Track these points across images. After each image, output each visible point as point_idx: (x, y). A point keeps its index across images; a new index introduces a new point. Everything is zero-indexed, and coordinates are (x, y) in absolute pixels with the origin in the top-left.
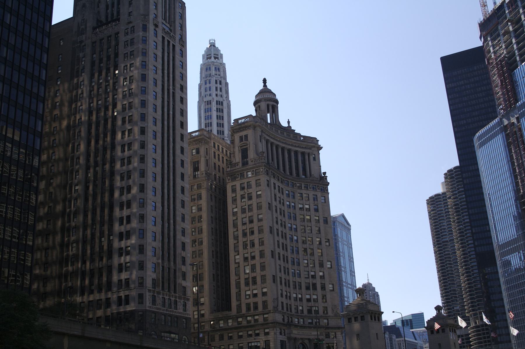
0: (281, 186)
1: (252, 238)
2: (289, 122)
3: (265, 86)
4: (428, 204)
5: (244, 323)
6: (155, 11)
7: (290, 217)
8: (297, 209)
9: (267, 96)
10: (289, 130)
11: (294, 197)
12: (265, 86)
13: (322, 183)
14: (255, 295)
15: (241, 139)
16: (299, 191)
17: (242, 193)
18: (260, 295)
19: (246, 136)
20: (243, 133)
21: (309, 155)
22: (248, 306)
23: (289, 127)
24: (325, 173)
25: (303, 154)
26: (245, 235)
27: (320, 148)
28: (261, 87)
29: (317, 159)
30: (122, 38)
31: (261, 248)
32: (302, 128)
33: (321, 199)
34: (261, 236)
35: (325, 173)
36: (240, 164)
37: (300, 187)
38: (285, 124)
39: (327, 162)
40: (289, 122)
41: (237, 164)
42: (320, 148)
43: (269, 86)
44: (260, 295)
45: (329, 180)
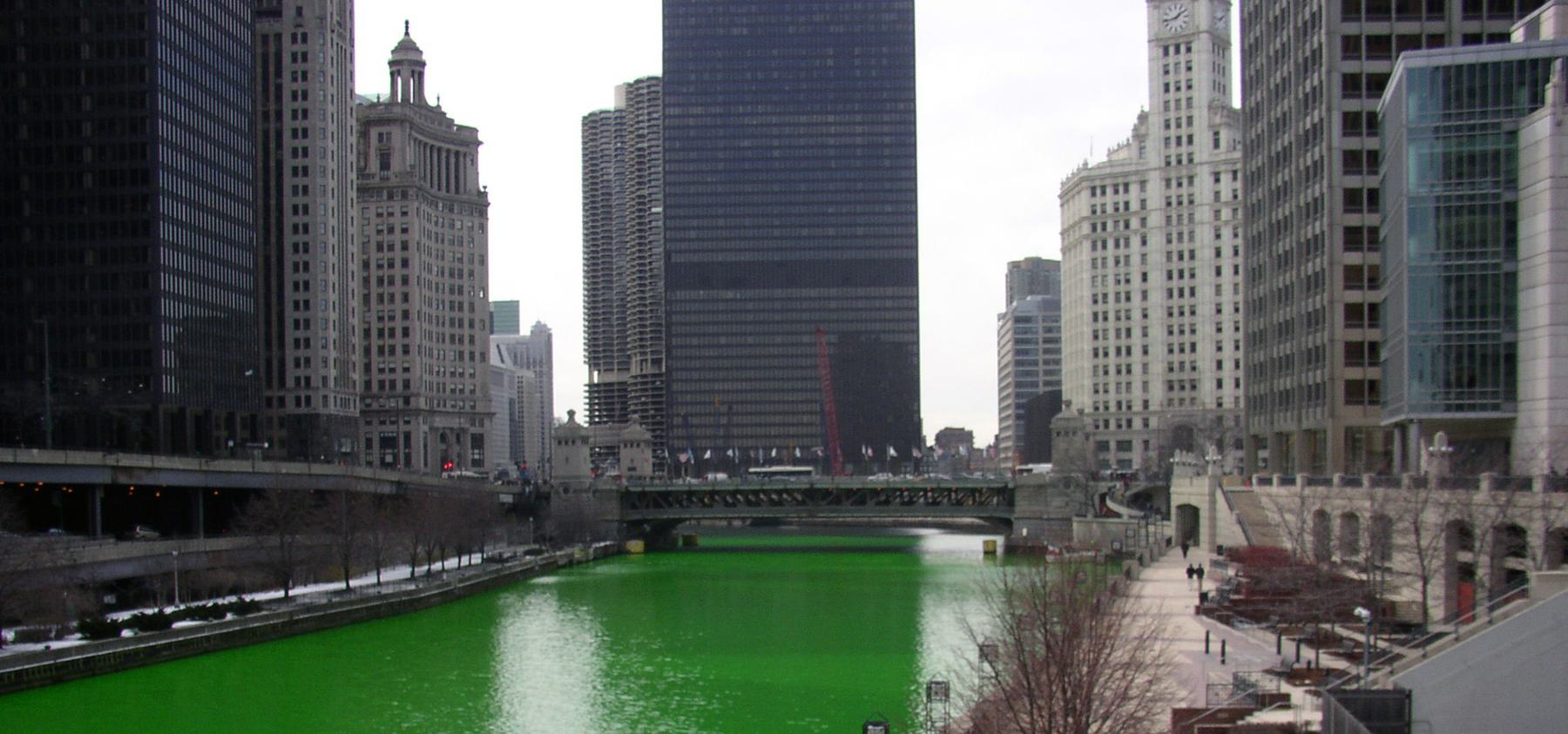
0: (428, 209)
1: (392, 290)
3: (407, 34)
4: (584, 125)
5: (375, 406)
6: (332, 8)
9: (412, 56)
10: (437, 114)
12: (407, 34)
14: (392, 370)
15: (381, 135)
18: (399, 370)
19: (389, 134)
20: (384, 130)
22: (382, 384)
23: (439, 106)
25: (457, 154)
26: (380, 281)
27: (480, 143)
28: (401, 36)
29: (474, 162)
30: (288, 48)
31: (405, 306)
32: (459, 114)
34: (405, 289)
36: (377, 179)
38: (432, 102)
39: (490, 171)
41: (373, 176)
42: (480, 143)
43: (413, 36)
44: (399, 370)
45: (490, 199)
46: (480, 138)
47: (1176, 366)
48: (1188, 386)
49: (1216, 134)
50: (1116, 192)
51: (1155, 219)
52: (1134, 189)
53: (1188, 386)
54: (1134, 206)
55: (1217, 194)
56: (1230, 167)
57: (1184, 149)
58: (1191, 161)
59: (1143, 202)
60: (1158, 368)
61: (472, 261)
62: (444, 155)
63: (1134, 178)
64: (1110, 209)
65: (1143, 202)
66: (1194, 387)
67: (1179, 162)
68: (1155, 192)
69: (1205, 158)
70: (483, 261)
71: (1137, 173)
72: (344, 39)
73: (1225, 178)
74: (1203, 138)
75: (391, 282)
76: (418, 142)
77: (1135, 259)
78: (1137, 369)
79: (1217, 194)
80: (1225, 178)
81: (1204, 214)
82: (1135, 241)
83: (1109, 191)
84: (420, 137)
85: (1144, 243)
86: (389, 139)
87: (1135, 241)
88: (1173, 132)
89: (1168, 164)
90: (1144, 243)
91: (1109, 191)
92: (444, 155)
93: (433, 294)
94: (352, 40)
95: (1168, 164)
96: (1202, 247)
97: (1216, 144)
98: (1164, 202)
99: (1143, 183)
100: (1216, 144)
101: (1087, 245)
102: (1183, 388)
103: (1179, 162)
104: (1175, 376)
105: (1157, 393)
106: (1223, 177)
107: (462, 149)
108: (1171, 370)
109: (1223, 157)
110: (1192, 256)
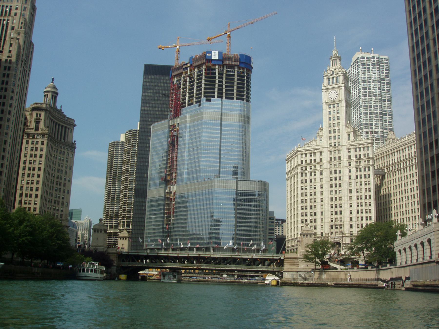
2: (61, 107)
7: (53, 163)
8: (58, 159)
10: (60, 112)
11: (57, 152)
13: (72, 147)
15: (37, 114)
16: (60, 149)
17: (32, 146)
20: (39, 112)
21: (69, 129)
23: (61, 110)
24: (75, 141)
25: (66, 127)
26: (30, 169)
27: (75, 126)
32: (68, 113)
33: (70, 156)
35: (75, 141)
37: (61, 148)
38: (59, 108)
39: (78, 135)
40: (61, 107)
42: (75, 126)
45: (77, 145)
46: (75, 123)
47: (334, 220)
48: (338, 227)
49: (349, 135)
50: (311, 156)
51: (326, 165)
52: (318, 155)
53: (338, 227)
54: (318, 161)
55: (350, 157)
56: (354, 147)
57: (337, 141)
58: (339, 145)
59: (321, 160)
60: (327, 221)
61: (66, 167)
62: (60, 127)
63: (318, 151)
64: (308, 162)
65: (321, 160)
66: (341, 228)
67: (335, 145)
68: (326, 156)
69: (345, 143)
70: (71, 168)
71: (319, 149)
72: (27, 66)
73: (353, 151)
74: (344, 137)
75: (34, 169)
76: (50, 118)
77: (318, 180)
78: (318, 221)
79: (350, 157)
80: (353, 151)
81: (345, 163)
82: (318, 173)
83: (308, 155)
84: (52, 118)
85: (321, 174)
86: (40, 116)
87: (318, 173)
88: (332, 135)
89: (331, 146)
90: (321, 174)
91: (308, 155)
92: (60, 127)
93: (50, 177)
94: (30, 68)
95: (331, 146)
96: (343, 176)
97: (349, 139)
98: (329, 159)
99: (321, 153)
100: (349, 139)
101: (300, 175)
102: (337, 228)
103: (335, 145)
104: (333, 224)
105: (327, 230)
106: (351, 150)
107: (68, 126)
108: (332, 221)
109: (351, 143)
110: (340, 178)
